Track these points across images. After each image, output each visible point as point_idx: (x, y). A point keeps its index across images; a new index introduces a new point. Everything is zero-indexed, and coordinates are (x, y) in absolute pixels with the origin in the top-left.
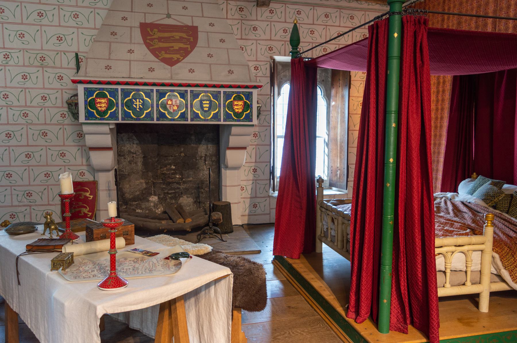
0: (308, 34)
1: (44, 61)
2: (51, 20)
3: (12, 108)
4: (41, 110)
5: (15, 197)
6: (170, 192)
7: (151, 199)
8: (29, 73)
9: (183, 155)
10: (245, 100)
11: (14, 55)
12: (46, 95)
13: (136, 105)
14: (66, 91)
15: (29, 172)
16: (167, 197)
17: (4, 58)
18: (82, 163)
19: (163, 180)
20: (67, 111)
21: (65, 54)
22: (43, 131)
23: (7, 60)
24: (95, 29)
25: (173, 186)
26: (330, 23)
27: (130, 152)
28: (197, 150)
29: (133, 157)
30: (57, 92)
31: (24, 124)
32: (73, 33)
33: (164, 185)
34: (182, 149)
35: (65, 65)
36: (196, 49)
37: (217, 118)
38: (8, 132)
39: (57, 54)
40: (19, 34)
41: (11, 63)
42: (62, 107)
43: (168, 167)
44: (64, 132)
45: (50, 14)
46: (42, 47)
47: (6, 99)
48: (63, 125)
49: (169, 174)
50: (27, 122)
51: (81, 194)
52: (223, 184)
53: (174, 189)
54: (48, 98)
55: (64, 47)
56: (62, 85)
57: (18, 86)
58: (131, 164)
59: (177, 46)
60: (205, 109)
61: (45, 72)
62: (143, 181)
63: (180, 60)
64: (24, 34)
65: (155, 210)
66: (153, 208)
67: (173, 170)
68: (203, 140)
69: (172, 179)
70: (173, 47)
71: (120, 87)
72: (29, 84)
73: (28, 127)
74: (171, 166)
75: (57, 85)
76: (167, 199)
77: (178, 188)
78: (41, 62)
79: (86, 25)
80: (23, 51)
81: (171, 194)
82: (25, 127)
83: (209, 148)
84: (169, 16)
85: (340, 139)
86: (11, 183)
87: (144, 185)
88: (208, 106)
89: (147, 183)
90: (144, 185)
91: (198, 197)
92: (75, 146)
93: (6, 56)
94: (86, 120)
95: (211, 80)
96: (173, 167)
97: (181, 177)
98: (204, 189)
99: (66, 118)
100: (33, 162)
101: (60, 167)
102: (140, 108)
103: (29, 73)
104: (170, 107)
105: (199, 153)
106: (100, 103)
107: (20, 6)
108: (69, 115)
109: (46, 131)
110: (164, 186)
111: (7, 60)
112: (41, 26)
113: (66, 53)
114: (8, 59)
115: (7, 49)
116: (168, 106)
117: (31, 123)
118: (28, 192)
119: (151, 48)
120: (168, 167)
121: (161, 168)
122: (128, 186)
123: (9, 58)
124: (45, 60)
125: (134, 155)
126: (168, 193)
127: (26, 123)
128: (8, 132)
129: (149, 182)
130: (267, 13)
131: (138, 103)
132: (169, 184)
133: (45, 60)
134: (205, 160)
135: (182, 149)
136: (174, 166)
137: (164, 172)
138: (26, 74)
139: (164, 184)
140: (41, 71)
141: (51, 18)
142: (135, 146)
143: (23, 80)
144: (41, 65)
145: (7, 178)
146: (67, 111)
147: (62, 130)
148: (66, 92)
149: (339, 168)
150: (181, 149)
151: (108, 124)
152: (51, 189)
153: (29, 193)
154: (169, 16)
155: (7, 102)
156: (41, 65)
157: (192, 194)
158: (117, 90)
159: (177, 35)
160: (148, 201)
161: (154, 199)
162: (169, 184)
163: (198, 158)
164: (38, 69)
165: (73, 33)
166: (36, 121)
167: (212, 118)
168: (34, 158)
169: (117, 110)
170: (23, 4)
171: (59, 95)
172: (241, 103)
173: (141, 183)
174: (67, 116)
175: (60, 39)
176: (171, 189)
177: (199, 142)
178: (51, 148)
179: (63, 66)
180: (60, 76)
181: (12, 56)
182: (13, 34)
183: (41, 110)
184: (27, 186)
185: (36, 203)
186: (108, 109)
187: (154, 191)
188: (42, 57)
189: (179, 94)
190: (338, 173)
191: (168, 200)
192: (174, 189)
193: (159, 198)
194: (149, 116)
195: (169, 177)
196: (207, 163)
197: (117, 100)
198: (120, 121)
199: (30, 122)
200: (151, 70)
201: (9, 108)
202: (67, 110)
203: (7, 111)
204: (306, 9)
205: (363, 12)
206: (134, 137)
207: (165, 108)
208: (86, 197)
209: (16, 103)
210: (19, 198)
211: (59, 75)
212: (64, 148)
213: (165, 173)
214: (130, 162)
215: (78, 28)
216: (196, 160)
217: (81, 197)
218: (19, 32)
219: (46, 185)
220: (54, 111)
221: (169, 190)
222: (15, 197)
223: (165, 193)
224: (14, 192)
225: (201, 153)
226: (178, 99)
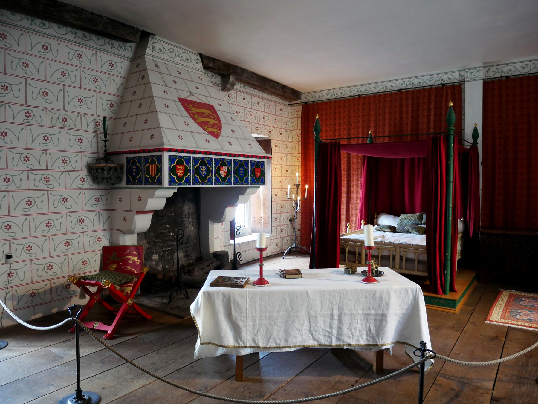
1: (66, 123)
2: (73, 80)
3: (32, 171)
4: (62, 174)
5: (34, 272)
6: (167, 249)
7: (153, 258)
8: (50, 134)
9: (173, 214)
10: (185, 164)
11: (37, 114)
12: (66, 159)
13: (202, 171)
14: (86, 154)
15: (49, 242)
17: (26, 116)
18: (99, 228)
20: (85, 176)
21: (85, 117)
22: (63, 197)
23: (28, 119)
24: (111, 94)
25: (169, 244)
26: (260, 109)
28: (182, 207)
30: (77, 155)
31: (44, 190)
32: (93, 96)
34: (173, 209)
35: (84, 128)
37: (247, 182)
38: (29, 198)
39: (78, 116)
40: (43, 92)
41: (33, 122)
42: (82, 171)
43: (164, 226)
44: (83, 198)
45: (72, 75)
46: (64, 108)
47: (26, 161)
48: (82, 189)
49: (165, 232)
50: (48, 187)
51: (130, 258)
52: (210, 237)
54: (68, 162)
55: (84, 109)
56: (81, 148)
57: (39, 147)
60: (241, 175)
61: (66, 133)
63: (219, 133)
64: (47, 93)
65: (157, 268)
66: (155, 266)
71: (192, 155)
72: (50, 146)
73: (49, 193)
74: (166, 226)
75: (77, 147)
76: (165, 257)
78: (63, 123)
79: (103, 90)
80: (46, 111)
82: (46, 192)
83: (190, 207)
84: (192, 94)
85: (263, 195)
86: (31, 256)
90: (147, 246)
91: (187, 251)
92: (93, 211)
93: (28, 115)
96: (167, 226)
98: (190, 244)
99: (85, 182)
100: (53, 231)
101: (79, 234)
103: (50, 134)
105: (184, 212)
106: (179, 169)
107: (44, 62)
108: (87, 180)
109: (66, 197)
110: (162, 244)
111: (28, 119)
112: (64, 85)
113: (85, 116)
114: (30, 118)
115: (29, 106)
117: (52, 189)
118: (48, 265)
119: (197, 121)
120: (164, 226)
121: (159, 227)
123: (31, 116)
124: (66, 121)
126: (166, 251)
127: (47, 188)
128: (29, 198)
129: (151, 242)
130: (227, 97)
131: (203, 170)
132: (166, 241)
133: (66, 121)
134: (189, 218)
135: (173, 209)
136: (168, 225)
138: (48, 135)
140: (62, 133)
141: (73, 79)
143: (44, 141)
144: (63, 126)
145: (27, 251)
146: (85, 176)
147: (81, 195)
148: (85, 156)
149: (262, 218)
152: (71, 259)
153: (50, 265)
155: (27, 165)
156: (63, 126)
157: (183, 249)
160: (152, 260)
161: (156, 257)
162: (166, 241)
164: (59, 130)
165: (93, 96)
166: (57, 186)
168: (54, 227)
170: (48, 61)
171: (78, 158)
172: (259, 170)
174: (85, 180)
175: (80, 101)
177: (184, 202)
178: (71, 214)
180: (80, 138)
181: (34, 115)
182: (36, 91)
183: (62, 174)
184: (48, 258)
185: (57, 276)
186: (185, 174)
187: (156, 250)
188: (64, 117)
190: (262, 221)
191: (166, 257)
195: (165, 235)
196: (190, 220)
199: (51, 187)
201: (29, 171)
202: (86, 173)
203: (28, 175)
205: (274, 104)
209: (37, 167)
210: (40, 273)
211: (79, 137)
212: (83, 214)
213: (163, 232)
215: (97, 92)
216: (183, 218)
217: (130, 261)
218: (43, 90)
219: (66, 255)
220: (73, 175)
221: (166, 248)
222: (34, 272)
223: (163, 251)
224: (34, 267)
226: (156, 164)
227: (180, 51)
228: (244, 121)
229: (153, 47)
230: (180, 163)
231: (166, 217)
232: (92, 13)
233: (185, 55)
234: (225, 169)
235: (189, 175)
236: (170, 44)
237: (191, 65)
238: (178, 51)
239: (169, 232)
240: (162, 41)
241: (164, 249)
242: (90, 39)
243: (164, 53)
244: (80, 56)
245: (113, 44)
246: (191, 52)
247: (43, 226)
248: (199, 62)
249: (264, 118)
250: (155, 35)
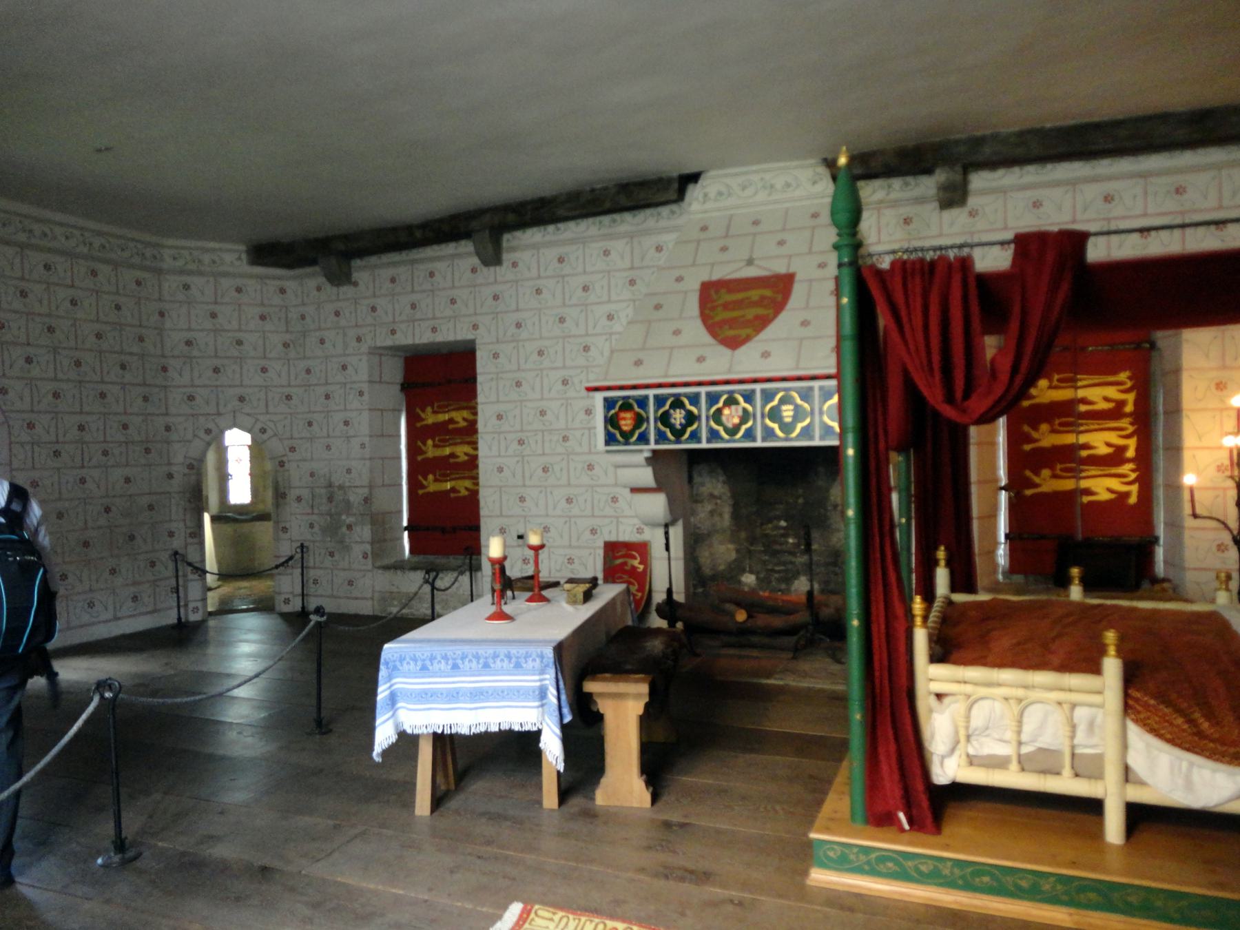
6: (777, 568)
9: (801, 501)
19: (764, 545)
27: (712, 496)
28: (828, 490)
29: (716, 504)
36: (783, 316)
53: (784, 564)
58: (712, 516)
59: (751, 313)
62: (731, 546)
67: (784, 528)
70: (743, 316)
76: (770, 582)
77: (791, 563)
81: (779, 572)
87: (733, 555)
88: (791, 413)
89: (738, 551)
95: (797, 368)
96: (783, 523)
102: (681, 424)
104: (728, 419)
105: (832, 498)
110: (767, 558)
116: (724, 419)
121: (762, 524)
122: (707, 554)
125: (719, 501)
126: (773, 570)
136: (786, 521)
139: (765, 552)
142: (720, 485)
151: (641, 451)
154: (750, 262)
158: (646, 397)
159: (755, 294)
163: (829, 508)
167: (798, 436)
173: (728, 549)
189: (743, 396)
191: (774, 583)
192: (784, 564)
193: (758, 578)
194: (749, 435)
197: (647, 412)
198: (653, 446)
200: (701, 359)
204: (1057, 193)
206: (720, 471)
207: (719, 422)
208: (634, 568)
214: (712, 513)
216: (826, 510)
223: (768, 570)
227: (767, 176)
229: (706, 195)
230: (626, 406)
231: (781, 506)
232: (593, 190)
233: (779, 182)
235: (646, 429)
236: (736, 175)
237: (798, 193)
238: (762, 179)
239: (786, 536)
240: (726, 176)
242: (622, 221)
243: (730, 195)
244: (606, 253)
245: (659, 214)
246: (796, 167)
247: (563, 503)
248: (821, 179)
250: (708, 171)
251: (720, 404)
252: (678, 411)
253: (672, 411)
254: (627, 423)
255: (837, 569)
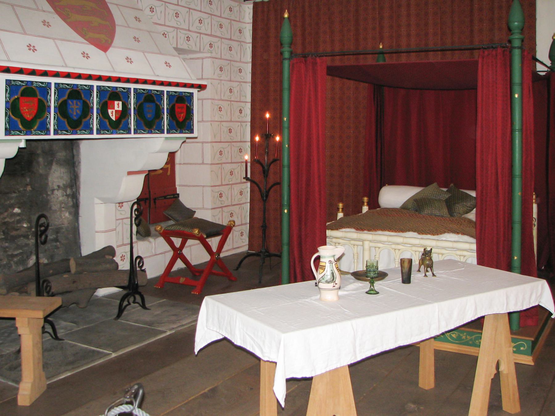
0: (173, 17)
6: (16, 253)
9: (29, 188)
16: (12, 262)
28: (46, 177)
33: (6, 243)
34: (28, 180)
43: (10, 210)
49: (13, 222)
67: (18, 215)
68: (54, 164)
69: (17, 230)
94: (6, 135)
96: (17, 210)
97: (29, 225)
105: (50, 184)
110: (7, 244)
120: (10, 210)
126: (13, 256)
136: (19, 208)
137: (6, 220)
139: (6, 239)
150: (26, 180)
157: (46, 251)
162: (13, 239)
163: (49, 193)
169: (49, 117)
176: (18, 247)
179: (222, 57)
191: (14, 267)
213: (7, 222)
216: (48, 195)
223: (8, 256)
225: (53, 184)
228: (165, 25)
231: (14, 195)
234: (118, 106)
241: (10, 253)
249: (200, 21)
251: (66, 97)
252: (75, 101)
253: (70, 102)
254: (28, 111)
255: (58, 243)
